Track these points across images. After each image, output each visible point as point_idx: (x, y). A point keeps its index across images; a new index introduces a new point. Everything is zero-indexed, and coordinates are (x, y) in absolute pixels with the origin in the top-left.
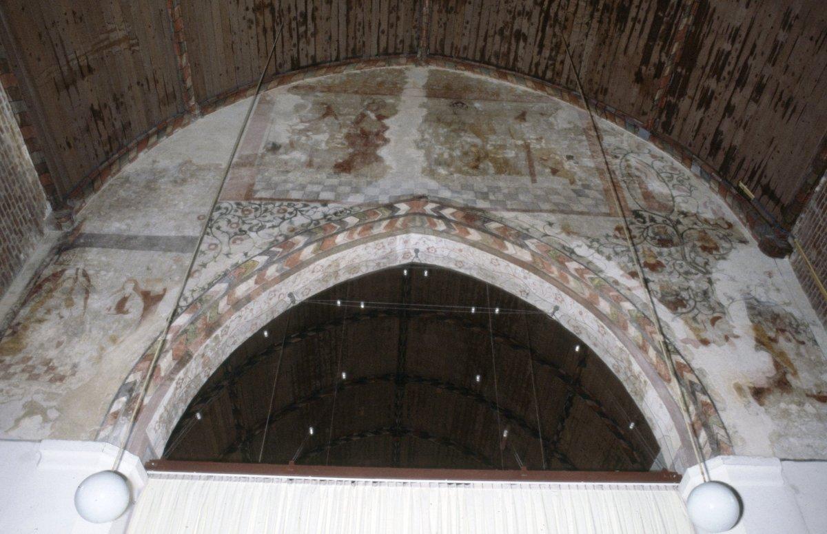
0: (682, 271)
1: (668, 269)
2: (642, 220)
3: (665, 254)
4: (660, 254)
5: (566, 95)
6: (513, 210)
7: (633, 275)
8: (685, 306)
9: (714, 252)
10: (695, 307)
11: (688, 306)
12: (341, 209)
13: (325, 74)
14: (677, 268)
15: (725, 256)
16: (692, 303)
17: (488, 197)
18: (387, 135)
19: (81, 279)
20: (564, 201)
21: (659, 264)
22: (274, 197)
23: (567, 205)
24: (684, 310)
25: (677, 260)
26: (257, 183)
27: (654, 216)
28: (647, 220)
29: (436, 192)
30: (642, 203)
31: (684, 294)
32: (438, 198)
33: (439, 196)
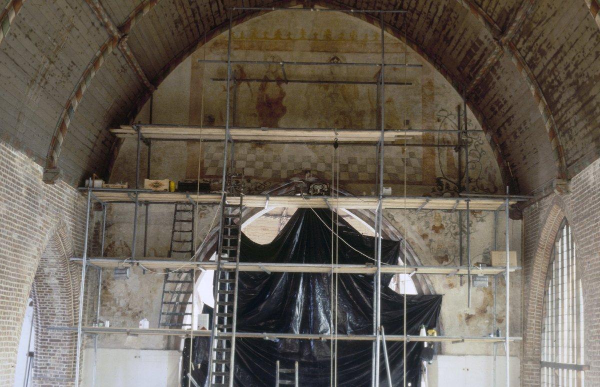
0: (454, 232)
1: (446, 231)
2: (440, 188)
3: (447, 218)
4: (445, 218)
5: (415, 47)
6: (363, 182)
7: (424, 236)
8: (447, 260)
9: (478, 215)
10: (453, 261)
11: (449, 260)
12: (259, 185)
13: (236, 25)
14: (452, 230)
15: (484, 218)
16: (452, 257)
17: (347, 169)
18: (284, 102)
19: (126, 249)
20: (395, 171)
21: (442, 227)
22: (218, 175)
23: (396, 175)
24: (446, 263)
25: (453, 223)
26: (205, 160)
27: (449, 183)
28: (444, 187)
29: (314, 165)
30: (445, 170)
31: (450, 251)
32: (317, 171)
33: (318, 170)
